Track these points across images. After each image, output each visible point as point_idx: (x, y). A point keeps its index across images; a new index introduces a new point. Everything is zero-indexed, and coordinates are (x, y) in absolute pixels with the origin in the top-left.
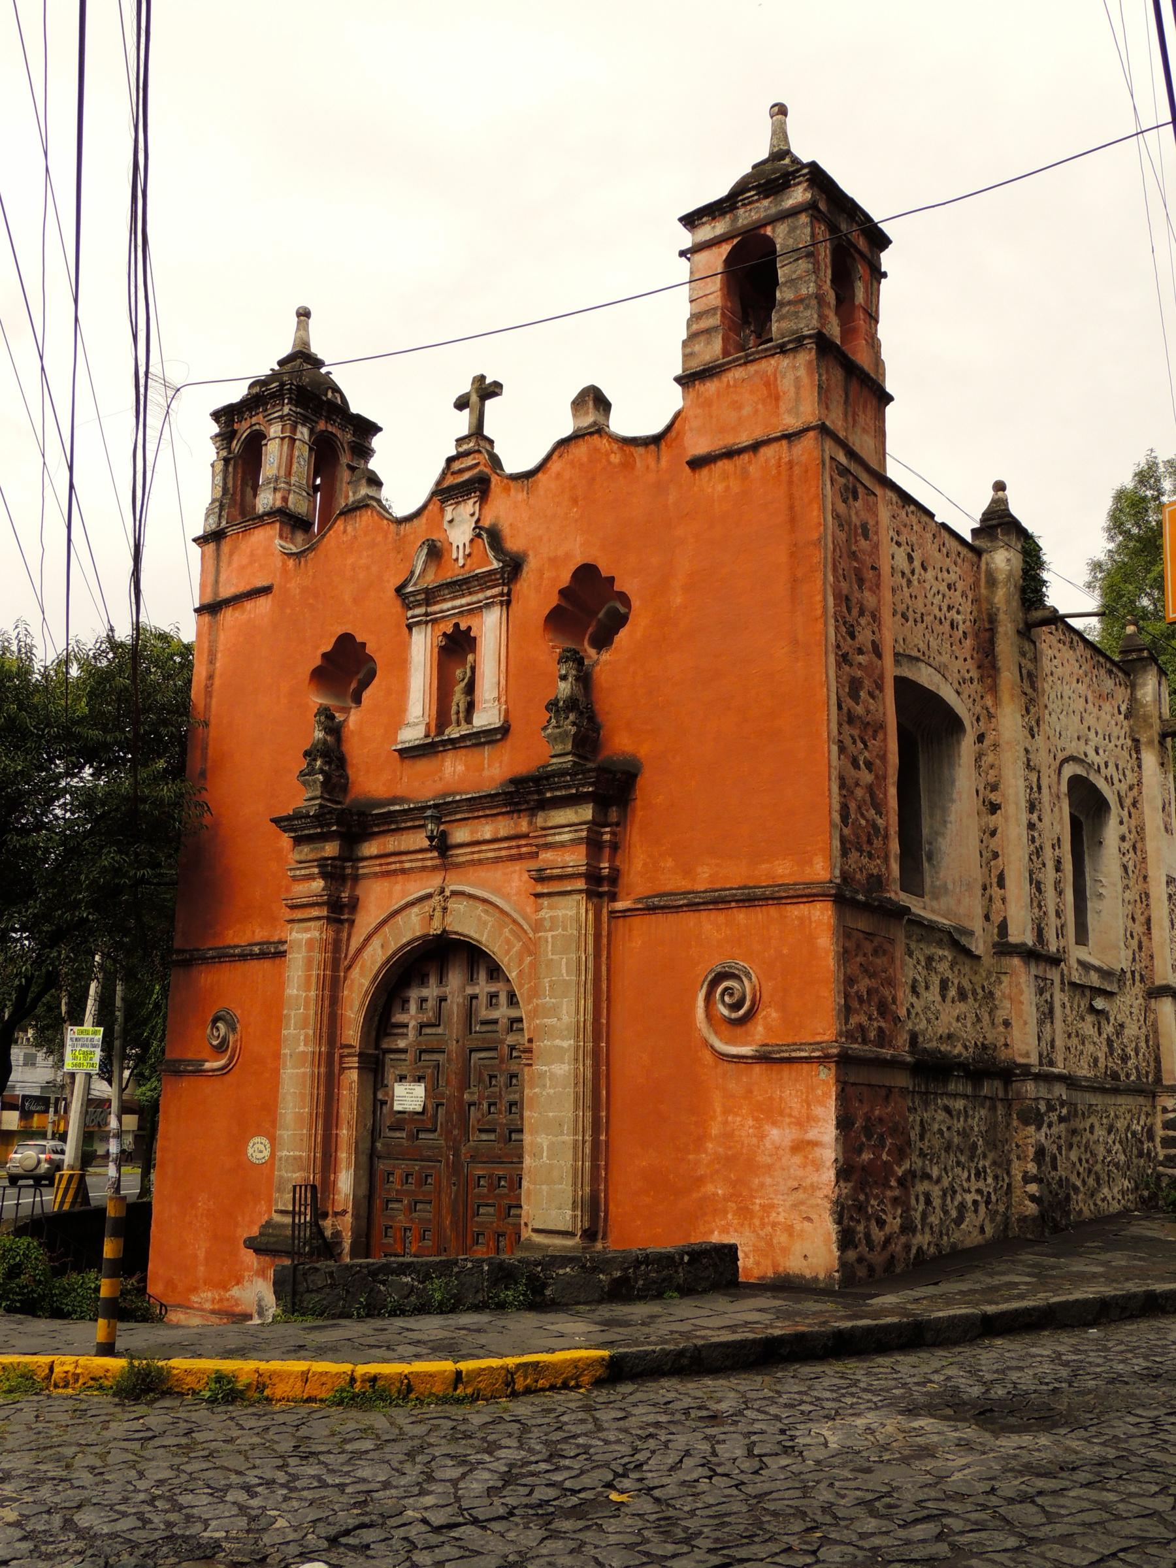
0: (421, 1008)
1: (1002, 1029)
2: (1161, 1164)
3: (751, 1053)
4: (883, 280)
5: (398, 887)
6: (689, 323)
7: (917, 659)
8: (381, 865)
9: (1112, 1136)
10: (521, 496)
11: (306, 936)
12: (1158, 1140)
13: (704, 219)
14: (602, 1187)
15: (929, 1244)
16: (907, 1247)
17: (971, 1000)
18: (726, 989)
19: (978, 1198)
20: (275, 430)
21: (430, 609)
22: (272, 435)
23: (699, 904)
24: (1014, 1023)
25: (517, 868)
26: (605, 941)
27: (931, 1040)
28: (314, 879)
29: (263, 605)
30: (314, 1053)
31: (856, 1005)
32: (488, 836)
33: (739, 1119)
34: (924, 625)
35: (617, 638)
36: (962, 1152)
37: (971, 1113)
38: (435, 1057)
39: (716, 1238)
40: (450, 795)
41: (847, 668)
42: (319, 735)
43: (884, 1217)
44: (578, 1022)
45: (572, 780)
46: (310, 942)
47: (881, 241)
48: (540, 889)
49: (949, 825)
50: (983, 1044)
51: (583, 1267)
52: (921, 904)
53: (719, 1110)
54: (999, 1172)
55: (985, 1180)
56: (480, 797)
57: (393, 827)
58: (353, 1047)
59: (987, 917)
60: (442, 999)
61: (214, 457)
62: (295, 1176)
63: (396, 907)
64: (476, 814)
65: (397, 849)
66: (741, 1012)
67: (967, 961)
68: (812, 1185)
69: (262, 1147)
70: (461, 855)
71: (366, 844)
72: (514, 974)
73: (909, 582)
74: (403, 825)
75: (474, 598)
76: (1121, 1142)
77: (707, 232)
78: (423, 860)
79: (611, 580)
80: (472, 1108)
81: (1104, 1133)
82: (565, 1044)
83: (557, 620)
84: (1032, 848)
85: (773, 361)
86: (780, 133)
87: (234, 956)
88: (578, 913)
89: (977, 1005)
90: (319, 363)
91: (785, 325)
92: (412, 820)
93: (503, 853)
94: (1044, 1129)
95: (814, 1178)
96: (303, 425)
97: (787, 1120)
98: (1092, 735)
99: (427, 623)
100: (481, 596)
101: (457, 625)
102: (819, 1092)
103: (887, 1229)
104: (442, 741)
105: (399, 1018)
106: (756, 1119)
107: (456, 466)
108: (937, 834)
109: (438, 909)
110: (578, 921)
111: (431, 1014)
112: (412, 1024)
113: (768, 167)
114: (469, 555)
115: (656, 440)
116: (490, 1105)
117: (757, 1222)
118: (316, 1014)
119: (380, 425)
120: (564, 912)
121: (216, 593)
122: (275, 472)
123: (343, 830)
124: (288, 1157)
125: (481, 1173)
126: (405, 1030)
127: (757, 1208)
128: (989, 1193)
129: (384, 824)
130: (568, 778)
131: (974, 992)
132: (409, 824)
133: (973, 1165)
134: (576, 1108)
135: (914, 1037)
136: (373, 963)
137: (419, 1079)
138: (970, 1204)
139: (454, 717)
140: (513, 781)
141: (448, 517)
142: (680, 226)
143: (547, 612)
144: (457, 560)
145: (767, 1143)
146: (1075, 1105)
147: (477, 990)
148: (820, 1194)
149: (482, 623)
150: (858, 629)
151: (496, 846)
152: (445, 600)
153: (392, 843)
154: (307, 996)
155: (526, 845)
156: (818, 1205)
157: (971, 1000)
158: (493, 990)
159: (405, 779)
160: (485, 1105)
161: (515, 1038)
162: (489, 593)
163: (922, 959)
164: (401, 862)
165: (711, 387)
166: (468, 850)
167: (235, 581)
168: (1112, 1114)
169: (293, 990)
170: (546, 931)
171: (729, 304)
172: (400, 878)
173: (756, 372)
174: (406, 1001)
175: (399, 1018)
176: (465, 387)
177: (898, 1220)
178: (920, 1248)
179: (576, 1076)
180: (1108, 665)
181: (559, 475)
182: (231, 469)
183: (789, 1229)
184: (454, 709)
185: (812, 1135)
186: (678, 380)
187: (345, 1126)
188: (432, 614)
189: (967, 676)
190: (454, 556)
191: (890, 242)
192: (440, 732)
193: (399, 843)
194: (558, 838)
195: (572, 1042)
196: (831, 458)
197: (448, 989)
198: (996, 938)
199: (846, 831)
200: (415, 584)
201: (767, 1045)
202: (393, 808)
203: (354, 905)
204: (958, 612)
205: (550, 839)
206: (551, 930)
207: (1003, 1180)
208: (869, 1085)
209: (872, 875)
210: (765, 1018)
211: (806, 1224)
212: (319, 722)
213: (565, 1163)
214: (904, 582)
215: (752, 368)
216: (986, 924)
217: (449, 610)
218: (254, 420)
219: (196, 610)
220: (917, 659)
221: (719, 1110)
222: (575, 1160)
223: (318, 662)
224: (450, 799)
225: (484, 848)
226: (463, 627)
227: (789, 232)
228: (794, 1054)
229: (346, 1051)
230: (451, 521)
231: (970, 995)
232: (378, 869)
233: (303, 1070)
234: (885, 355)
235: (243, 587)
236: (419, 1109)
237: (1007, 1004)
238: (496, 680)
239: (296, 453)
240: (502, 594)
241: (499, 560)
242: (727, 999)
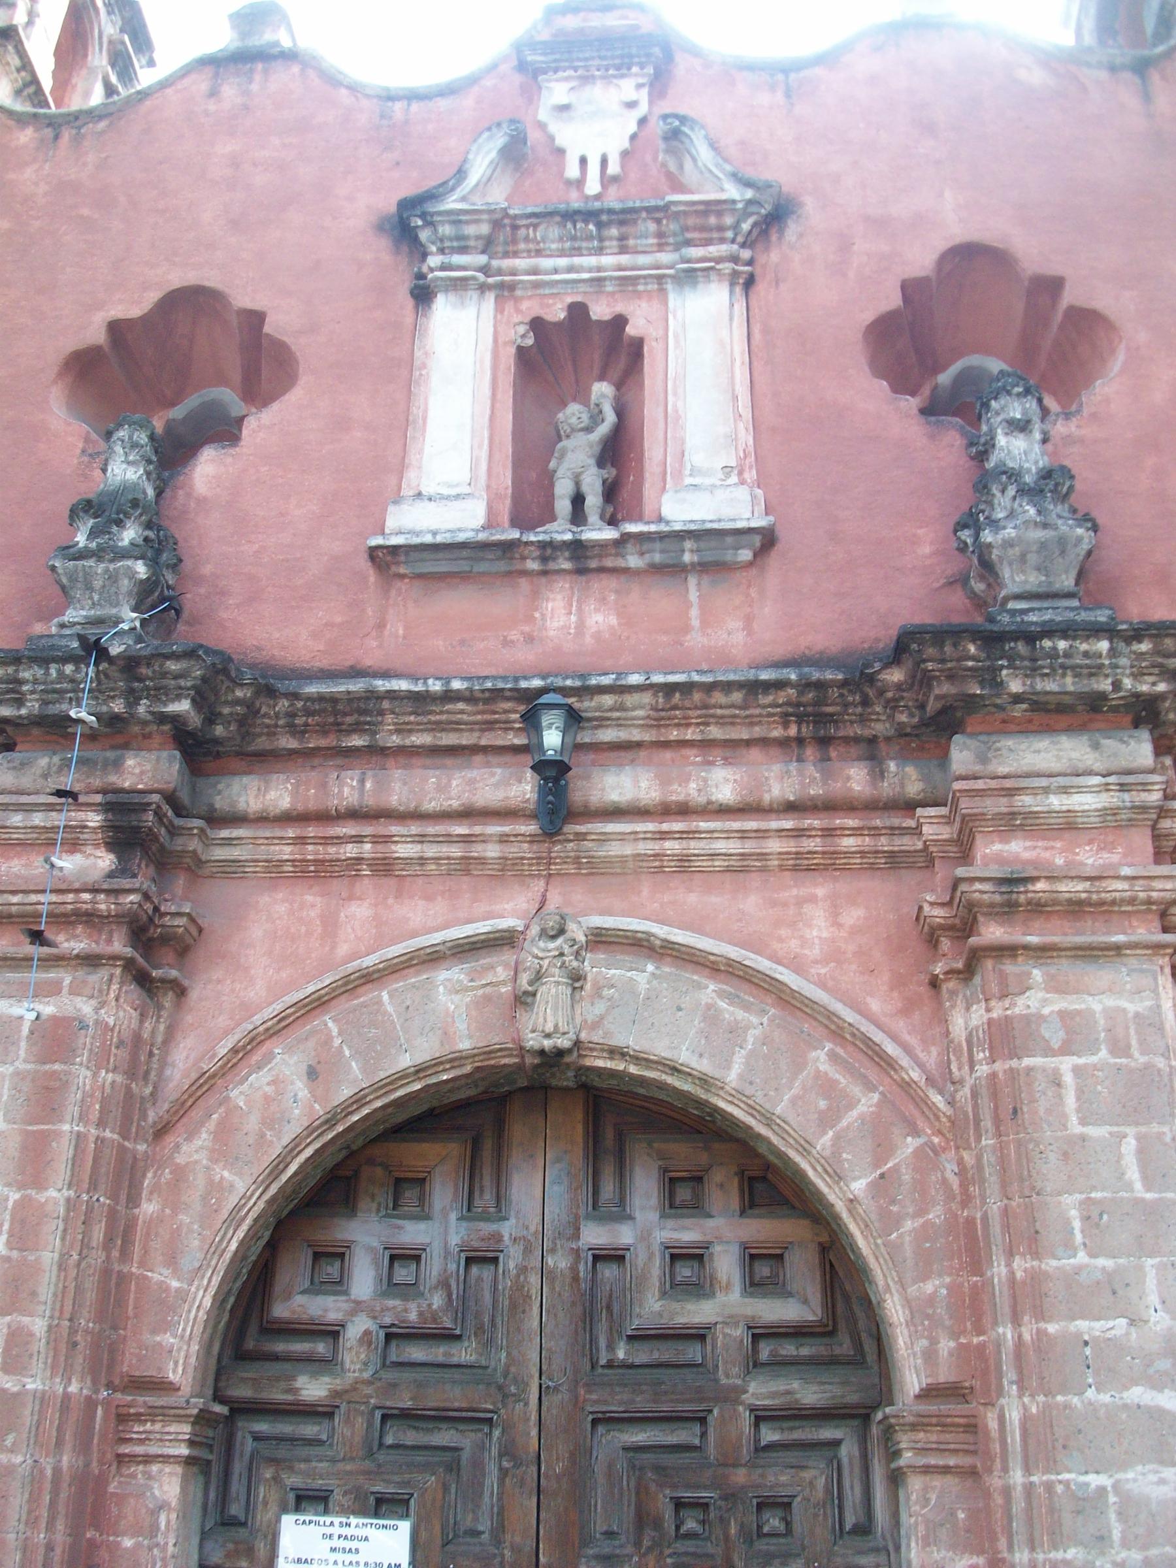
8: (301, 841)
21: (495, 263)
25: (820, 892)
28: (73, 846)
38: (444, 1437)
45: (1113, 652)
56: (710, 688)
57: (357, 741)
58: (163, 1386)
63: (369, 961)
64: (674, 734)
65: (370, 801)
72: (859, 1186)
74: (395, 740)
78: (467, 839)
92: (438, 727)
93: (774, 846)
99: (483, 288)
109: (557, 975)
114: (615, 179)
118: (62, 1266)
120: (1110, 1002)
123: (195, 720)
126: (321, 1348)
129: (324, 731)
130: (1104, 645)
132: (418, 739)
136: (270, 1122)
143: (869, 316)
144: (580, 183)
147: (625, 1235)
151: (752, 825)
154: (21, 1205)
155: (856, 832)
158: (687, 1233)
159: (396, 628)
161: (780, 1385)
164: (387, 839)
166: (650, 826)
170: (1049, 1052)
172: (366, 885)
184: (563, 489)
188: (500, 272)
190: (573, 171)
193: (380, 785)
194: (1056, 802)
197: (507, 1229)
200: (463, 199)
202: (381, 685)
205: (1025, 801)
217: (556, 271)
223: (96, 334)
224: (606, 680)
225: (703, 825)
229: (143, 1401)
232: (286, 852)
240: (735, 259)
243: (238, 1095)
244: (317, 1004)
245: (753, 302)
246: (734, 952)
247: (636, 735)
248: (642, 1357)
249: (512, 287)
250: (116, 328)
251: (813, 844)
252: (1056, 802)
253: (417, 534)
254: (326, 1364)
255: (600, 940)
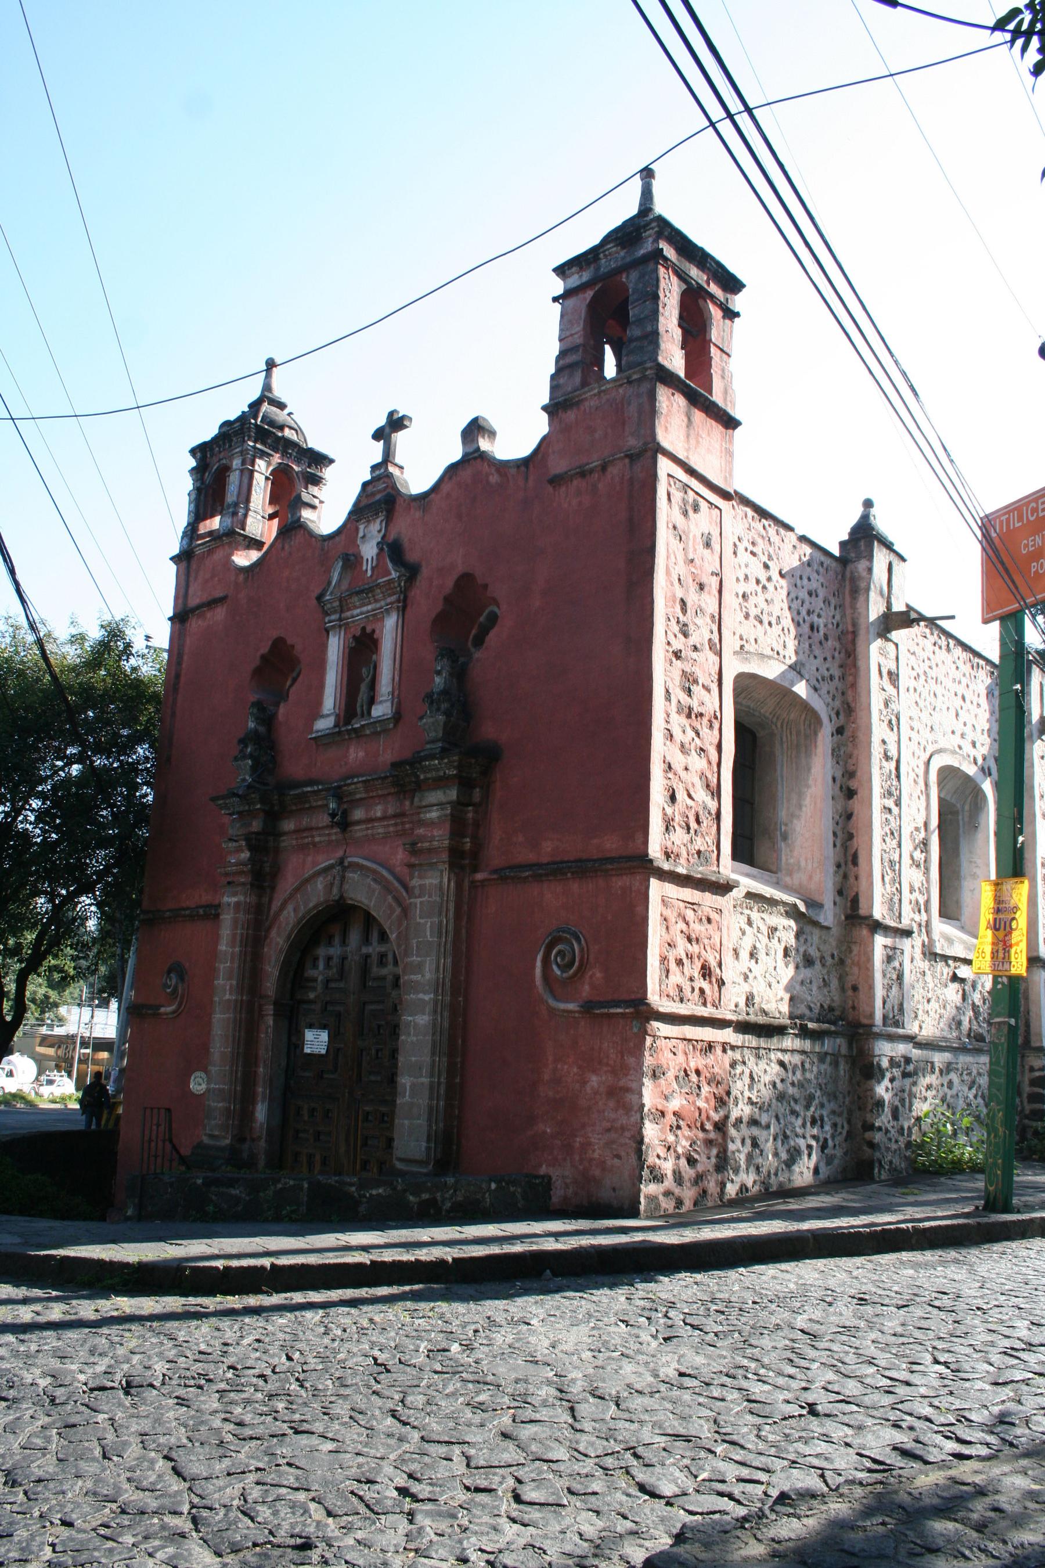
0: (328, 966)
1: (850, 993)
2: (1027, 1117)
3: (577, 1009)
4: (736, 320)
5: (310, 859)
6: (558, 359)
7: (769, 657)
9: (974, 1091)
10: (418, 514)
11: (234, 899)
12: (1025, 1095)
13: (574, 269)
14: (455, 1123)
15: (755, 1182)
16: (723, 1185)
17: (818, 966)
18: (559, 952)
19: (814, 1143)
20: (236, 463)
22: (234, 466)
23: (541, 875)
24: (860, 987)
26: (465, 908)
27: (768, 1002)
28: (242, 851)
29: (219, 614)
30: (236, 1001)
31: (673, 966)
32: (379, 814)
33: (566, 1067)
34: (780, 627)
35: (487, 639)
36: (796, 1101)
37: (807, 1066)
39: (543, 1170)
40: (348, 778)
41: (678, 664)
42: (251, 725)
43: (696, 1156)
44: (438, 978)
46: (237, 904)
47: (732, 284)
48: (414, 860)
49: (804, 809)
50: (829, 1007)
51: (394, 1189)
52: (775, 880)
53: (551, 1058)
54: (839, 1120)
55: (822, 1127)
57: (307, 806)
59: (840, 892)
60: (344, 959)
61: (191, 487)
62: (221, 1105)
66: (572, 971)
67: (816, 932)
68: (622, 1125)
69: (200, 1081)
70: (359, 831)
71: (286, 821)
73: (764, 587)
74: (314, 804)
75: (378, 605)
76: (983, 1097)
77: (575, 281)
78: (329, 835)
79: (485, 586)
80: (364, 1053)
81: (966, 1089)
82: (427, 998)
83: (441, 621)
84: (887, 829)
85: (621, 391)
86: (647, 195)
87: (184, 916)
88: (441, 882)
89: (825, 971)
90: (282, 406)
91: (631, 358)
93: (391, 829)
94: (886, 1082)
95: (624, 1120)
96: (260, 458)
97: (605, 1069)
98: (968, 730)
99: (340, 626)
100: (383, 603)
101: (364, 629)
102: (632, 1044)
103: (700, 1168)
104: (347, 730)
105: (311, 973)
106: (580, 1067)
107: (370, 489)
108: (793, 815)
110: (441, 888)
111: (335, 970)
112: (320, 978)
113: (636, 220)
115: (525, 463)
116: (377, 1051)
117: (577, 1158)
119: (331, 456)
120: (430, 881)
121: (185, 603)
122: (235, 499)
124: (214, 1089)
125: (367, 1108)
127: (578, 1144)
128: (826, 1140)
131: (822, 958)
133: (809, 1114)
134: (433, 1054)
135: (750, 1000)
137: (323, 1027)
138: (803, 1148)
139: (359, 710)
140: (394, 765)
141: (361, 534)
142: (554, 274)
145: (588, 1090)
146: (932, 1063)
147: (370, 950)
148: (627, 1134)
149: (383, 626)
150: (691, 627)
152: (356, 607)
153: (305, 821)
154: (233, 953)
156: (626, 1144)
157: (818, 966)
159: (319, 764)
160: (373, 1052)
162: (389, 600)
163: (764, 929)
164: (313, 837)
165: (571, 416)
167: (199, 593)
168: (975, 1072)
169: (223, 947)
171: (592, 342)
173: (608, 400)
174: (316, 959)
175: (311, 973)
176: (382, 421)
177: (713, 1160)
178: (743, 1188)
179: (434, 1025)
180: (988, 668)
181: (448, 495)
182: (202, 498)
183: (602, 1164)
184: (358, 704)
185: (621, 1083)
186: (545, 408)
187: (261, 1065)
189: (826, 674)
190: (364, 568)
191: (744, 286)
192: (348, 722)
194: (428, 816)
195: (432, 996)
196: (669, 475)
197: (349, 949)
198: (849, 912)
199: (669, 811)
201: (591, 1001)
203: (276, 872)
204: (819, 616)
206: (420, 896)
207: (843, 1127)
208: (685, 1039)
209: (699, 852)
210: (591, 977)
211: (616, 1160)
212: (252, 714)
213: (423, 1101)
214: (759, 589)
215: (604, 398)
216: (838, 899)
218: (221, 456)
219: (170, 619)
220: (769, 657)
221: (551, 1058)
222: (431, 1098)
223: (257, 662)
224: (349, 781)
226: (369, 630)
227: (640, 278)
228: (612, 1011)
230: (364, 537)
231: (818, 962)
232: (294, 842)
233: (227, 1016)
234: (736, 385)
235: (205, 597)
236: (323, 1052)
237: (855, 970)
238: (390, 676)
239: (255, 482)
241: (396, 571)
242: (559, 959)
243: (281, 918)
244: (297, 890)
245: (406, 616)
246: (374, 866)
247: (363, 795)
248: (375, 985)
249: (347, 624)
250: (263, 657)
251: (400, 828)
252: (428, 816)
253: (317, 731)
254: (314, 989)
255: (351, 864)
